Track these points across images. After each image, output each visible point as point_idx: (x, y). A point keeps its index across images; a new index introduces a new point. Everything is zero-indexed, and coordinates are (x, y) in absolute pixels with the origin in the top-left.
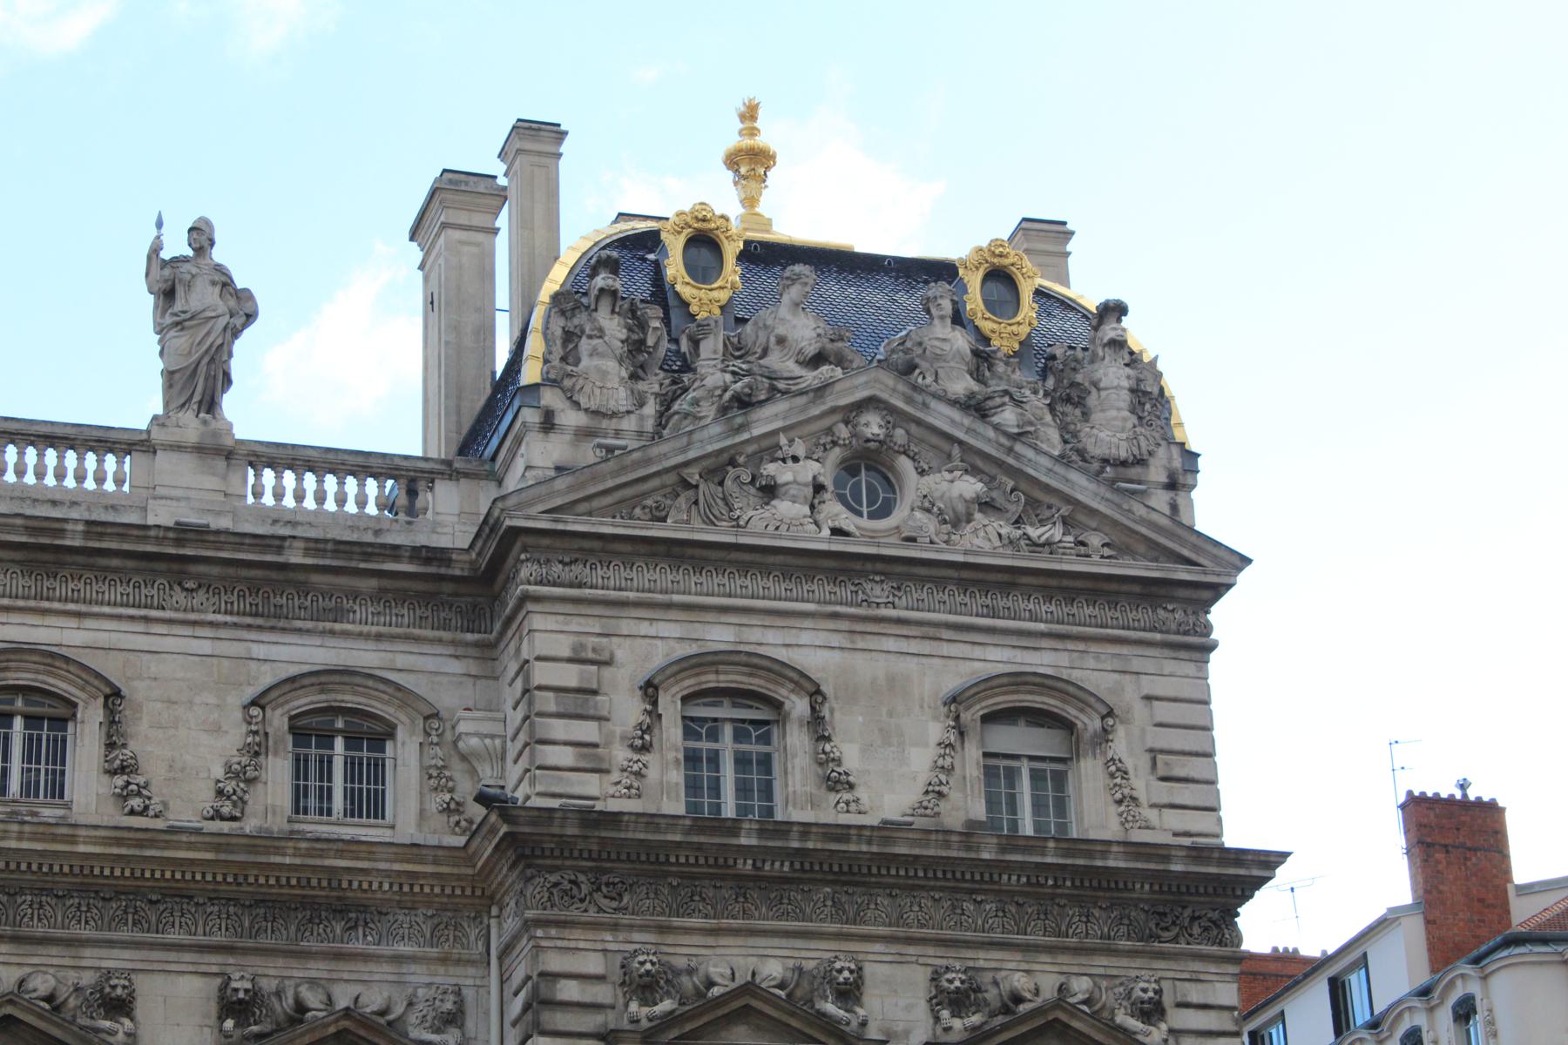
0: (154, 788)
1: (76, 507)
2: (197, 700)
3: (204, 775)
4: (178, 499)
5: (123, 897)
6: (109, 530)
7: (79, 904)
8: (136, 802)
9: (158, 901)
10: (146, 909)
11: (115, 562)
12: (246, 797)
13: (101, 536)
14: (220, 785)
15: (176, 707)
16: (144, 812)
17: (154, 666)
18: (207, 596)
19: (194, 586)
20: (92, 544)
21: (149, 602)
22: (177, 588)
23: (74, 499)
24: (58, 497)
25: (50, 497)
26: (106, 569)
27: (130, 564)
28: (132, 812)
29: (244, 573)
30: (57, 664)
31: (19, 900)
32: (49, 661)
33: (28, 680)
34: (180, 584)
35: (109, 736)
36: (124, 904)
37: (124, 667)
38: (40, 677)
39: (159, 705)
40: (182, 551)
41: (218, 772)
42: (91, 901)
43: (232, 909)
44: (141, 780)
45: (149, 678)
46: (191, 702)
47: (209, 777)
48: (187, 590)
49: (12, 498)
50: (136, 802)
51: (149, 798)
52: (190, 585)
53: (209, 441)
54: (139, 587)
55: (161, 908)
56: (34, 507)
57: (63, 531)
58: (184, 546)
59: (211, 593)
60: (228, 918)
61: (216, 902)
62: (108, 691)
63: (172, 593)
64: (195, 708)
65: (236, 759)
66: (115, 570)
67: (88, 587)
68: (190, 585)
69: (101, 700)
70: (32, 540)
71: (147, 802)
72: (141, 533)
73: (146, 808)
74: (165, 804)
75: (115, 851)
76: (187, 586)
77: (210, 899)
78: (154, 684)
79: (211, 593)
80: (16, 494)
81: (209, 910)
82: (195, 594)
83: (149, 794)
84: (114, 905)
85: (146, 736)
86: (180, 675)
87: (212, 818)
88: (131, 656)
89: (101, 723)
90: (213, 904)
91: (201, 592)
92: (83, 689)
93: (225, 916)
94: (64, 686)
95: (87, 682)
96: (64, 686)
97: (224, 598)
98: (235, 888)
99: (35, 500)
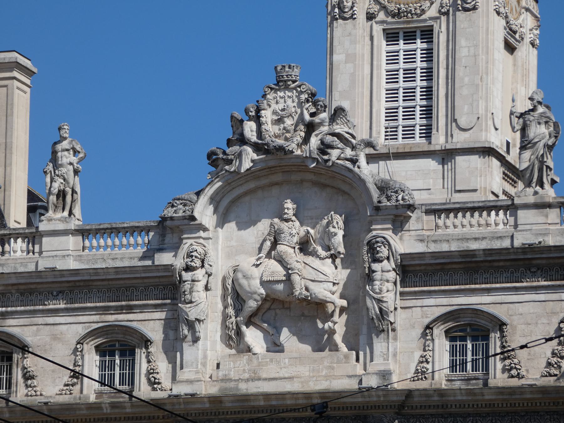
0: (522, 364)
1: (485, 240)
2: (539, 322)
3: (543, 356)
4: (526, 230)
5: (510, 414)
6: (493, 252)
7: (492, 419)
8: (514, 372)
9: (524, 415)
10: (520, 419)
11: (501, 264)
12: (561, 364)
13: (491, 255)
14: (549, 361)
15: (530, 326)
16: (519, 376)
17: (520, 308)
18: (541, 274)
19: (535, 270)
20: (490, 259)
21: (517, 279)
22: (528, 272)
23: (484, 236)
24: (477, 236)
25: (474, 236)
26: (498, 267)
27: (508, 264)
28: (513, 377)
29: (557, 261)
30: (479, 313)
31: (468, 420)
32: (475, 312)
33: (469, 321)
34: (530, 270)
35: (502, 343)
36: (510, 417)
37: (508, 310)
38: (473, 319)
39: (523, 326)
40: (526, 257)
41: (549, 354)
42: (497, 418)
43: (555, 416)
44: (516, 361)
45: (519, 314)
46: (537, 323)
47: (546, 357)
48: (532, 272)
49: (458, 240)
50: (514, 372)
51: (520, 369)
52: (533, 270)
53: (539, 201)
54: (513, 273)
55: (526, 418)
56: (468, 242)
57: (475, 255)
58: (527, 254)
59: (544, 272)
60: (554, 420)
61: (549, 413)
62: (500, 323)
63: (526, 274)
64: (539, 325)
65: (556, 348)
66: (502, 267)
67: (491, 275)
68: (533, 270)
69: (498, 327)
70: (463, 260)
71: (519, 371)
72: (507, 251)
73: (518, 374)
74: (527, 371)
75: (501, 397)
76: (532, 270)
77: (547, 412)
78: (521, 316)
79: (544, 272)
80: (460, 237)
81: (546, 418)
82: (536, 274)
83: (520, 368)
84: (506, 419)
85: (518, 341)
86: (532, 311)
87: (546, 376)
88: (511, 305)
89: (499, 338)
90: (548, 415)
91: (540, 271)
92: (491, 323)
93: (552, 420)
94: (483, 322)
95: (492, 320)
96: (483, 322)
97: (549, 273)
98: (555, 407)
99: (468, 239)
